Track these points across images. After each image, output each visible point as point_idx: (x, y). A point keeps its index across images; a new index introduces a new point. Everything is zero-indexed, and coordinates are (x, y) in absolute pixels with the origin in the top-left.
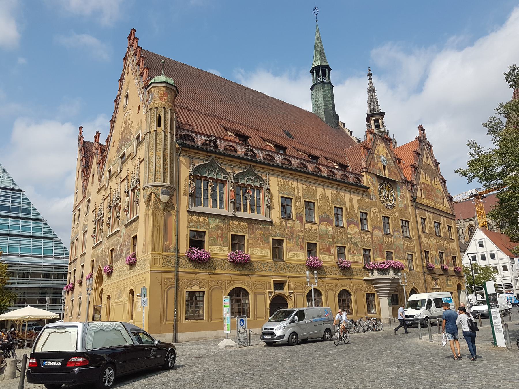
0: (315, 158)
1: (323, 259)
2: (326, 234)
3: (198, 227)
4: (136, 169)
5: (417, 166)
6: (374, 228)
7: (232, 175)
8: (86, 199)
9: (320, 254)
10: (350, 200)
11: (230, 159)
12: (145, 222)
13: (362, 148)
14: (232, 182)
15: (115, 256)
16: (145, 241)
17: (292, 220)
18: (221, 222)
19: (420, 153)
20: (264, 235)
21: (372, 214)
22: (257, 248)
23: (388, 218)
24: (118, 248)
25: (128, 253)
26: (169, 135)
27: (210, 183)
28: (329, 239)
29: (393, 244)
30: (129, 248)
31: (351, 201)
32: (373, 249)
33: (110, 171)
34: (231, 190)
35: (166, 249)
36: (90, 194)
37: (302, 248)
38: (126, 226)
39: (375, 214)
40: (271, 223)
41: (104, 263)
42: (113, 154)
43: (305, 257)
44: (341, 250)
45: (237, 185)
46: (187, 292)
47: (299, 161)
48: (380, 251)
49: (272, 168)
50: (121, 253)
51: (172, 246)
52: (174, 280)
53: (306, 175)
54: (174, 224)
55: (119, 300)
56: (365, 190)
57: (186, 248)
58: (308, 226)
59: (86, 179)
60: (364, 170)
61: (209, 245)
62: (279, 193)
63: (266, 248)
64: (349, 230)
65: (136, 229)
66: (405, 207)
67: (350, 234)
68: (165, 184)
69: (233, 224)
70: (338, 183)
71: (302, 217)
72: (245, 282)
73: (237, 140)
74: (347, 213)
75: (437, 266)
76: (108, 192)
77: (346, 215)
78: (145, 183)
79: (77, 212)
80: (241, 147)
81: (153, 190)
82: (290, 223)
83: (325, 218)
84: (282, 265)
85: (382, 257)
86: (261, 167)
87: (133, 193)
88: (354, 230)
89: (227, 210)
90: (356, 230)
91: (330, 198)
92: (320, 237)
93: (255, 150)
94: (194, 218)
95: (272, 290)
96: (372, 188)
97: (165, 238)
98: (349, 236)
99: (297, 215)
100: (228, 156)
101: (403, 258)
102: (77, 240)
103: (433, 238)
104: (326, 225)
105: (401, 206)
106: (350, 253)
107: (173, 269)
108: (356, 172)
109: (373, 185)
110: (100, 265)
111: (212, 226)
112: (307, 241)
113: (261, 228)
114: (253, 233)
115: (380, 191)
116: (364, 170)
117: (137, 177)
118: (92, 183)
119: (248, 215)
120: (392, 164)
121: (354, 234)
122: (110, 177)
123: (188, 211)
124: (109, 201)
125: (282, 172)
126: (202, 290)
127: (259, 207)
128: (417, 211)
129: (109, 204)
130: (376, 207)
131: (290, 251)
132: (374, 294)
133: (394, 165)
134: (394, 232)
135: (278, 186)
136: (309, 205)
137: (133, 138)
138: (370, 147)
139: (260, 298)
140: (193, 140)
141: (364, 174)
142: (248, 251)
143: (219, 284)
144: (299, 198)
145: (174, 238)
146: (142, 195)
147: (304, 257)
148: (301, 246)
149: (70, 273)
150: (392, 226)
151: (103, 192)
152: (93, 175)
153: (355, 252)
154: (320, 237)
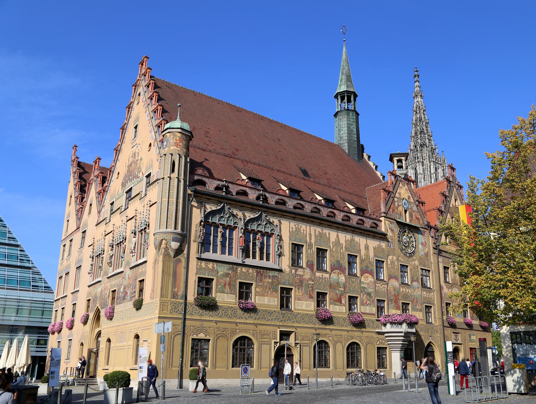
0: (330, 202)
1: (333, 309)
2: (338, 283)
3: (207, 274)
4: (145, 211)
5: (443, 210)
6: (390, 277)
7: (243, 221)
8: (81, 230)
9: (330, 304)
10: (365, 246)
11: (242, 205)
12: (154, 268)
13: (382, 191)
14: (242, 228)
15: (117, 298)
16: (154, 286)
17: (302, 267)
18: (229, 270)
19: (447, 195)
21: (389, 262)
22: (264, 296)
23: (407, 266)
24: (122, 290)
25: (133, 297)
26: (182, 181)
27: (220, 229)
28: (340, 289)
29: (411, 295)
30: (135, 292)
31: (367, 248)
32: (388, 300)
33: (112, 204)
34: (241, 237)
35: (174, 296)
36: (86, 225)
37: (311, 297)
38: (131, 268)
39: (392, 262)
40: (281, 271)
41: (104, 305)
42: (115, 185)
43: (314, 307)
44: (352, 300)
45: (246, 232)
46: (192, 339)
47: (313, 206)
48: (396, 302)
50: (124, 296)
51: (181, 293)
52: (180, 327)
53: (319, 221)
54: (183, 271)
55: (121, 344)
56: (383, 237)
57: (194, 295)
58: (318, 274)
59: (82, 208)
60: (383, 215)
61: (216, 292)
62: (290, 240)
63: (274, 297)
64: (363, 279)
65: (144, 273)
66: (427, 255)
67: (363, 283)
68: (176, 231)
69: (241, 271)
70: (353, 229)
71: (313, 265)
72: (251, 331)
73: (249, 184)
74: (362, 261)
75: (459, 320)
76: (110, 228)
77: (361, 264)
78: (156, 229)
79: (68, 243)
80: (253, 191)
81: (165, 236)
82: (300, 272)
83: (337, 267)
84: (289, 315)
85: (398, 308)
87: (140, 234)
88: (368, 280)
89: (236, 257)
90: (371, 279)
91: (344, 245)
92: (331, 286)
93: (267, 195)
94: (203, 264)
95: (278, 340)
96: (390, 234)
97: (174, 285)
98: (362, 285)
99: (307, 263)
100: (240, 202)
101: (421, 310)
102: (67, 274)
103: (457, 289)
104: (339, 274)
105: (422, 253)
106: (362, 304)
107: (181, 316)
108: (374, 217)
109: (392, 231)
110: (98, 305)
111: (220, 273)
112: (317, 290)
113: (269, 276)
114: (261, 281)
115: (399, 237)
116: (383, 215)
117: (147, 220)
118: (90, 213)
119: (256, 262)
120: (415, 208)
121: (368, 284)
122: (112, 210)
123: (197, 258)
124: (111, 238)
126: (208, 337)
127: (268, 255)
128: (441, 259)
129: (111, 242)
130: (394, 254)
131: (299, 300)
132: (386, 348)
133: (416, 209)
134: (412, 282)
135: (290, 232)
136: (321, 253)
137: (142, 176)
138: (391, 190)
139: (265, 347)
140: (204, 184)
141: (382, 219)
142: (255, 300)
143: (224, 333)
144: (310, 245)
145: (182, 285)
146: (151, 240)
147: (313, 306)
148: (310, 295)
149: (56, 311)
150: (411, 276)
151: (102, 226)
152: (91, 205)
153: (368, 303)
154: (331, 286)
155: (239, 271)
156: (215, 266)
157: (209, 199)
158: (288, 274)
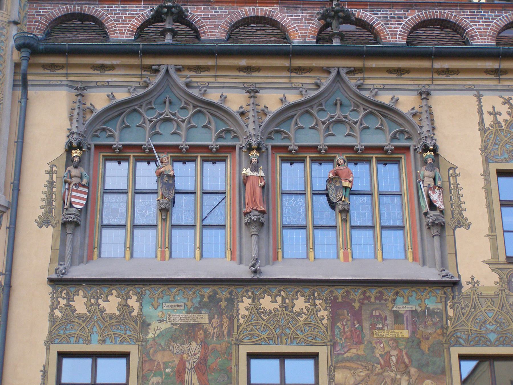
3: (95, 337)
11: (243, 62)
18: (198, 310)
20: (414, 342)
49: (439, 64)
62: (487, 160)
69: (256, 309)
86: (390, 71)
94: (80, 304)
111: (157, 327)
113: (398, 317)
114: (357, 338)
123: (52, 281)
125: (497, 72)
135: (482, 129)
140: (98, 25)
155: (242, 311)
156: (133, 302)
157: (103, 67)
158: (491, 299)
